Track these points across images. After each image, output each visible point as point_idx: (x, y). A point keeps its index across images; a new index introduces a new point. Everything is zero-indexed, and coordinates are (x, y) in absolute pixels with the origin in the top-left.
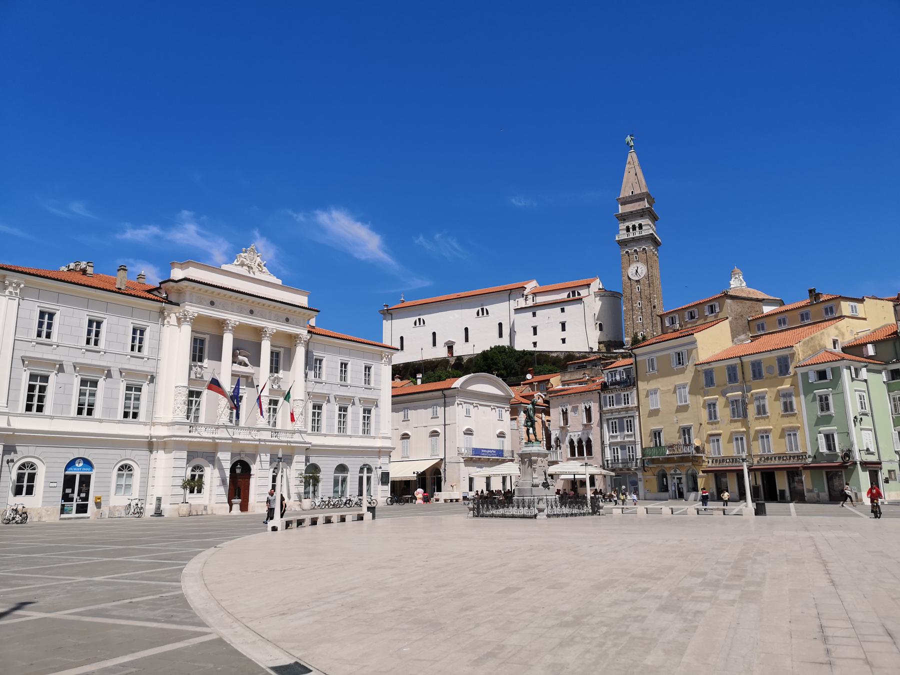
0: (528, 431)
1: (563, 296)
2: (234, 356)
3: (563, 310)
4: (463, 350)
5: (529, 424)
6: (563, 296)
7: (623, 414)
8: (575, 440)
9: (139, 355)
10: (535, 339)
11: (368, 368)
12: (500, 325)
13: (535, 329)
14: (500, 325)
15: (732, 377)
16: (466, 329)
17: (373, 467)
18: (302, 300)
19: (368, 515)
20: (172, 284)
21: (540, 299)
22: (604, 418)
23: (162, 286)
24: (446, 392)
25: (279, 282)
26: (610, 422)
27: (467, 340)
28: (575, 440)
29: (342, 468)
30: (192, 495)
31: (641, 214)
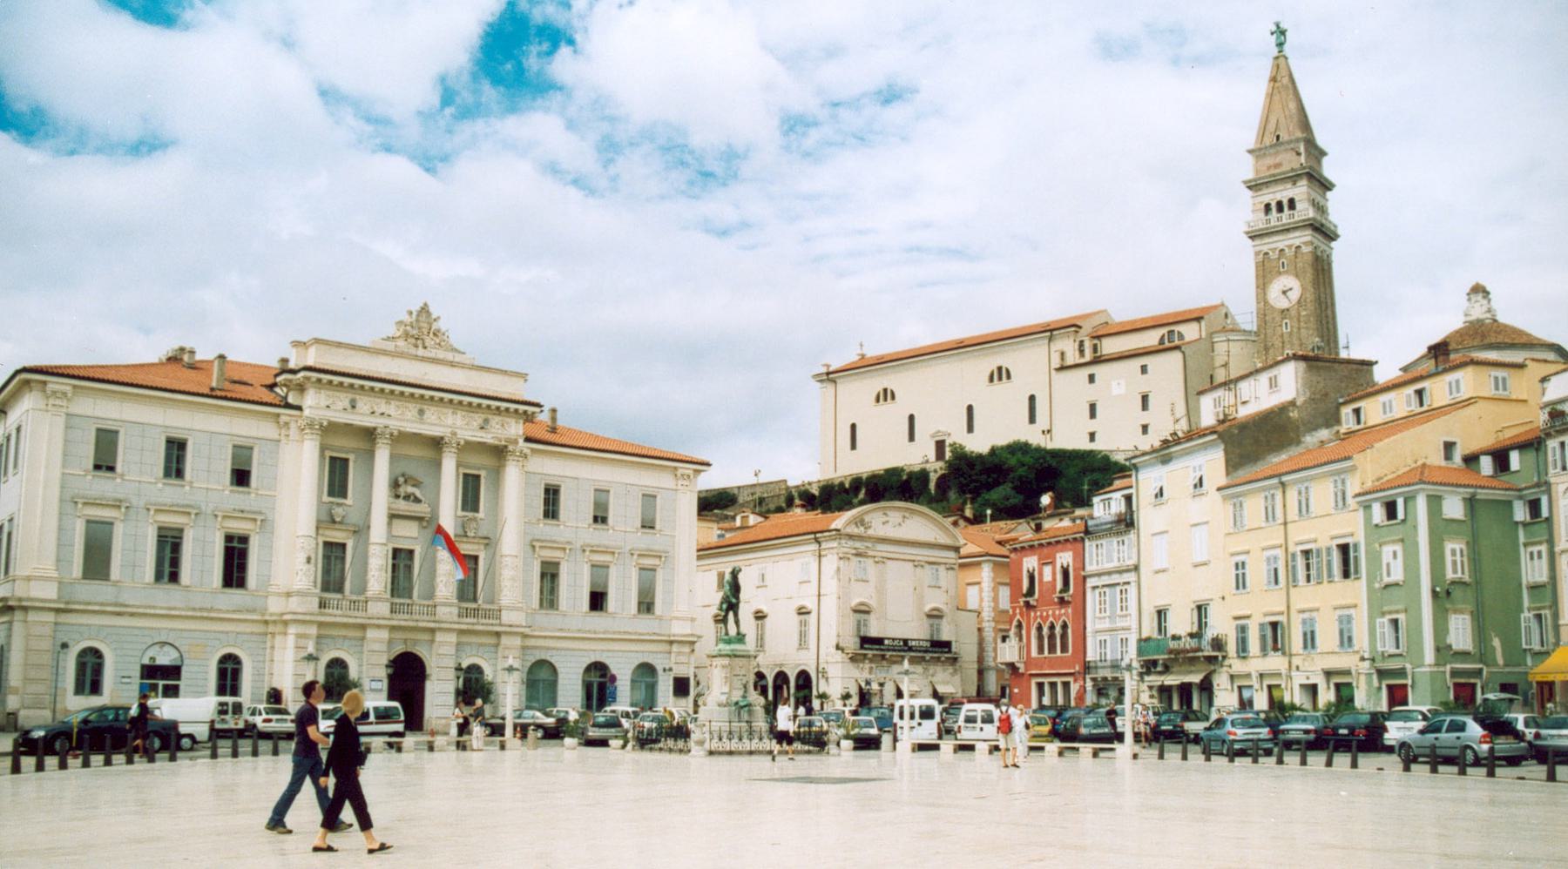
1: (1151, 339)
2: (395, 485)
3: (1144, 369)
6: (1151, 339)
7: (1115, 579)
10: (1092, 425)
11: (649, 498)
12: (1032, 398)
13: (1093, 408)
14: (1032, 398)
15: (1269, 515)
17: (659, 668)
20: (289, 376)
21: (1110, 346)
23: (279, 379)
31: (1293, 179)
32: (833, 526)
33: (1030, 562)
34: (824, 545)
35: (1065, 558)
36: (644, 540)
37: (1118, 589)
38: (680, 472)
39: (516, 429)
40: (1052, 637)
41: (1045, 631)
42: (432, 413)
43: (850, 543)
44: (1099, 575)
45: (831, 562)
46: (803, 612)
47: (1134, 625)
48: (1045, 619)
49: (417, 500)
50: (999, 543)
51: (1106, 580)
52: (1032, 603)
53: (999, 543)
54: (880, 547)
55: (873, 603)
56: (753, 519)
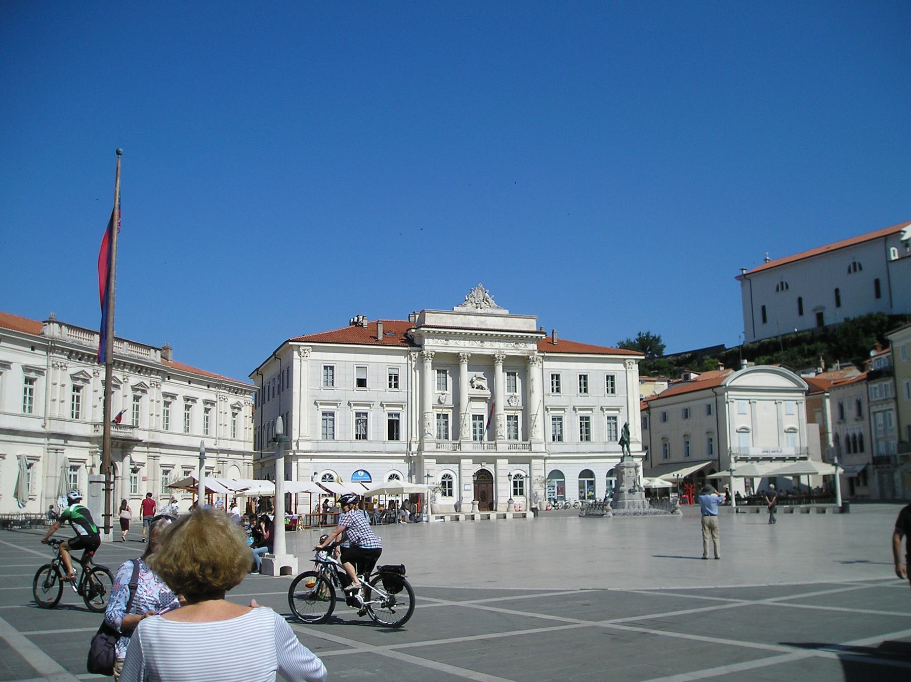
2: (472, 382)
4: (833, 318)
8: (851, 436)
9: (396, 389)
11: (611, 378)
12: (877, 282)
14: (877, 282)
16: (837, 291)
18: (530, 324)
19: (530, 515)
22: (872, 411)
24: (715, 390)
25: (506, 312)
27: (838, 304)
28: (851, 436)
29: (587, 473)
30: (445, 498)
36: (610, 400)
38: (627, 362)
39: (533, 347)
40: (855, 443)
42: (487, 344)
47: (897, 434)
49: (482, 388)
51: (880, 408)
55: (750, 427)
56: (693, 376)
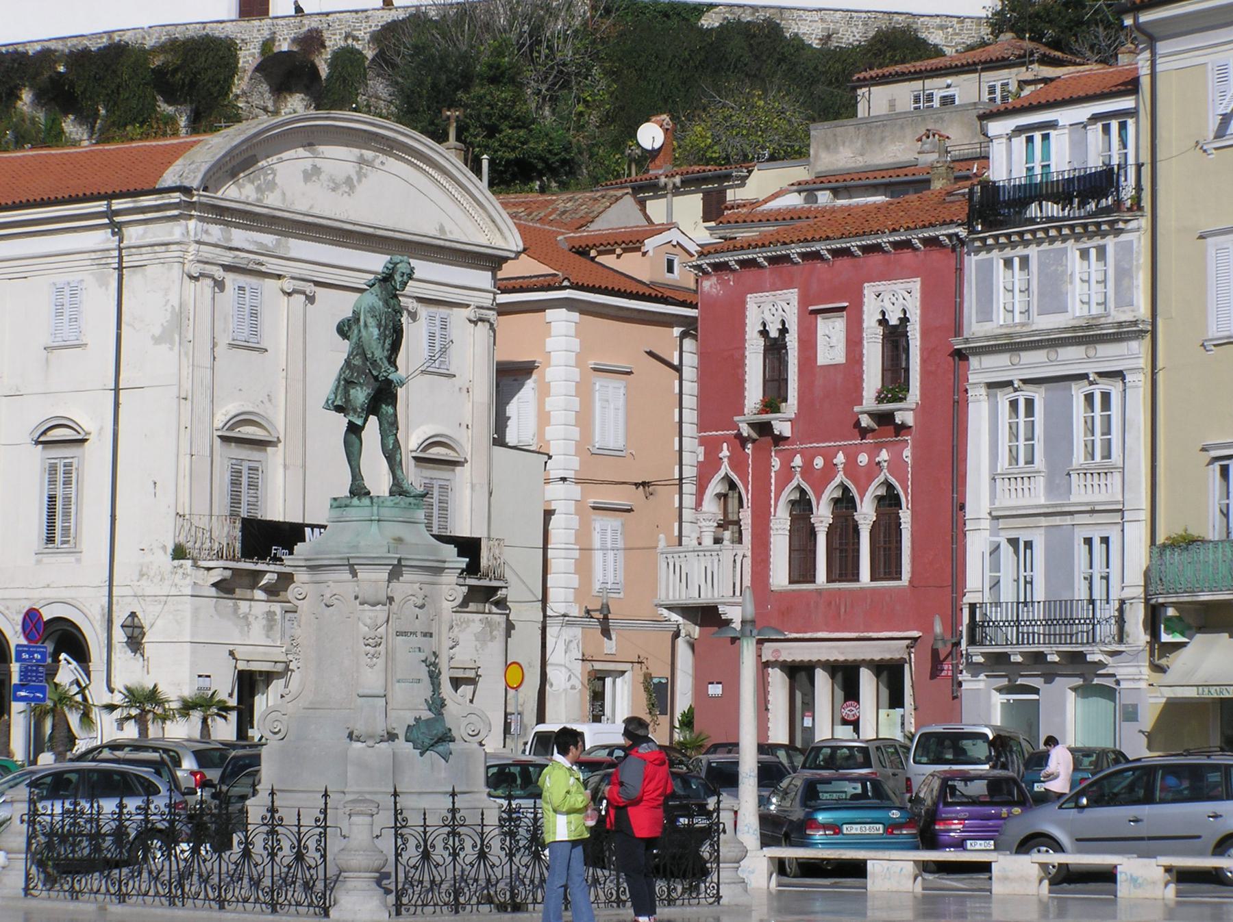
0: (354, 430)
5: (360, 395)
26: (1004, 398)
32: (169, 178)
33: (771, 309)
34: (133, 234)
35: (895, 298)
37: (1078, 392)
40: (844, 530)
41: (823, 515)
43: (215, 232)
44: (1012, 345)
45: (158, 291)
46: (59, 439)
48: (821, 480)
50: (582, 252)
51: (1036, 363)
52: (782, 427)
53: (582, 252)
54: (300, 248)
